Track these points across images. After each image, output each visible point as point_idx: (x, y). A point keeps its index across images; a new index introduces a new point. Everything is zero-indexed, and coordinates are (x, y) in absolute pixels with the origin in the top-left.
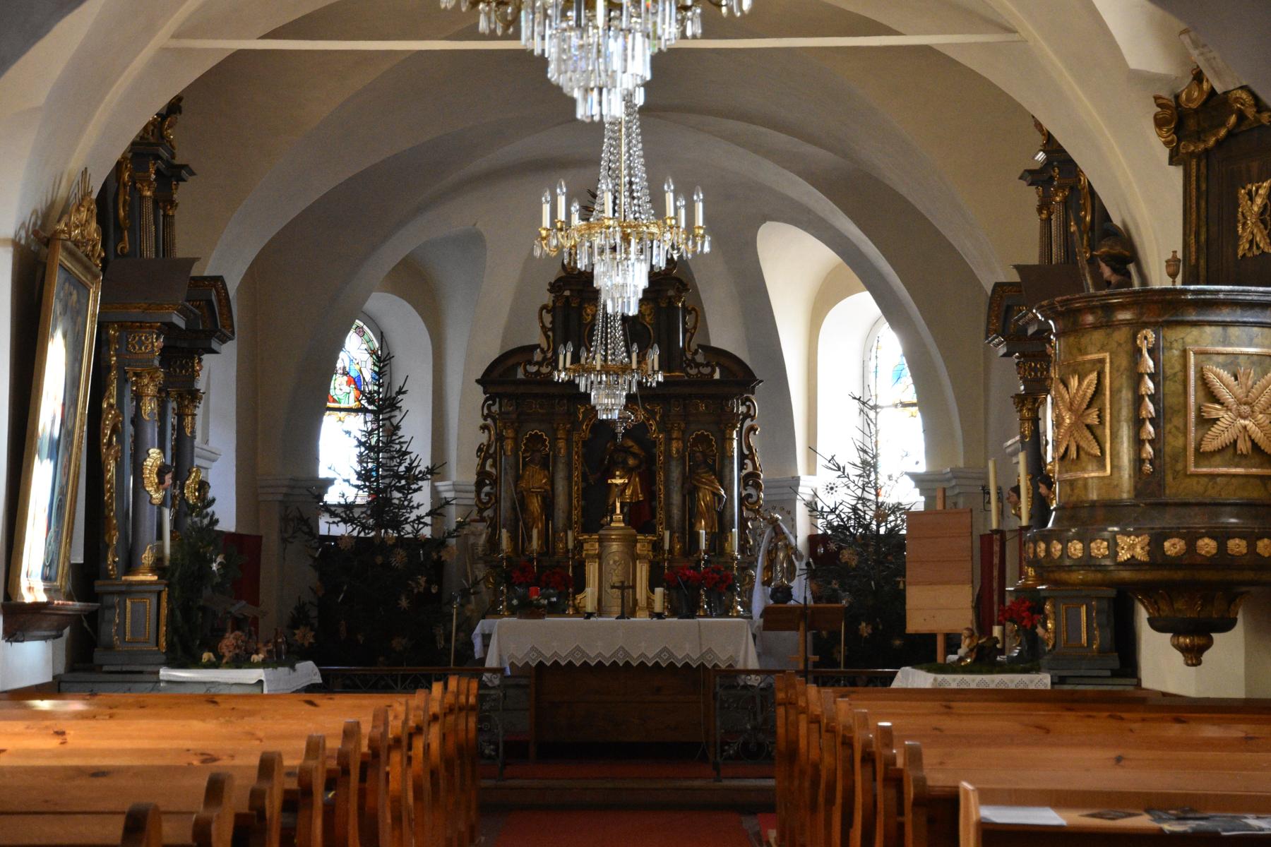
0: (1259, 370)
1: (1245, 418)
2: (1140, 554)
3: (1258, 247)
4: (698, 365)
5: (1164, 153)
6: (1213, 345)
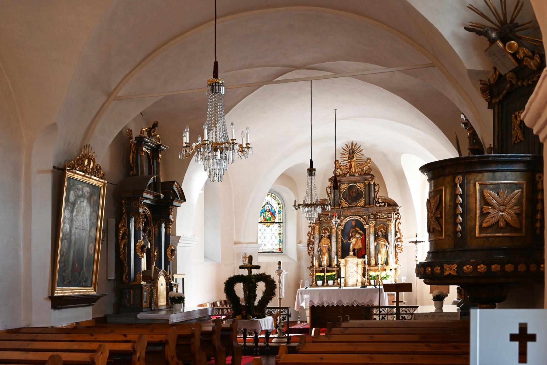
0: (510, 190)
1: (502, 212)
2: (454, 273)
3: (519, 139)
4: (380, 203)
5: (486, 104)
6: (488, 181)
